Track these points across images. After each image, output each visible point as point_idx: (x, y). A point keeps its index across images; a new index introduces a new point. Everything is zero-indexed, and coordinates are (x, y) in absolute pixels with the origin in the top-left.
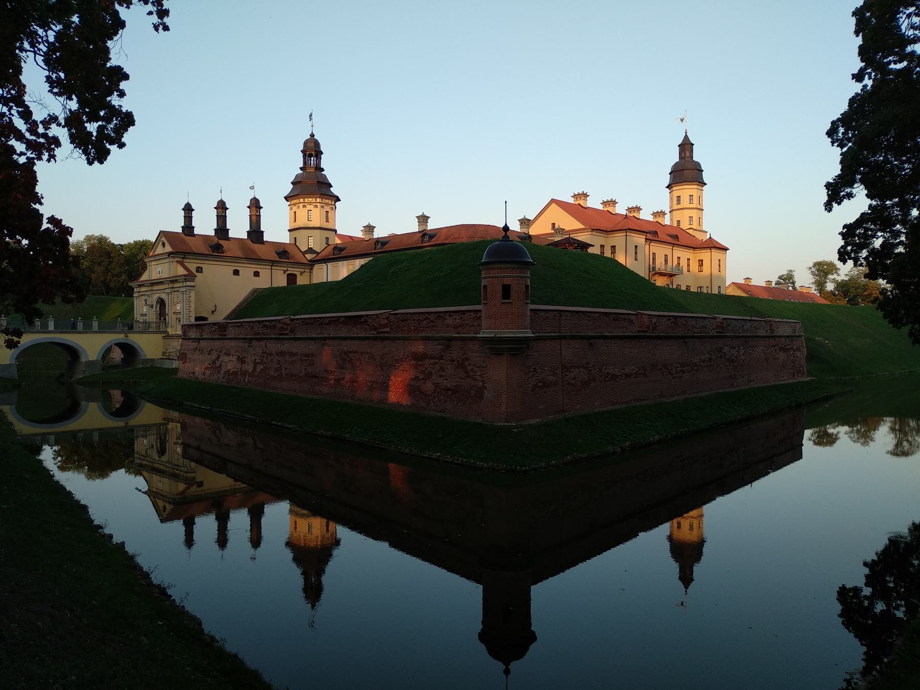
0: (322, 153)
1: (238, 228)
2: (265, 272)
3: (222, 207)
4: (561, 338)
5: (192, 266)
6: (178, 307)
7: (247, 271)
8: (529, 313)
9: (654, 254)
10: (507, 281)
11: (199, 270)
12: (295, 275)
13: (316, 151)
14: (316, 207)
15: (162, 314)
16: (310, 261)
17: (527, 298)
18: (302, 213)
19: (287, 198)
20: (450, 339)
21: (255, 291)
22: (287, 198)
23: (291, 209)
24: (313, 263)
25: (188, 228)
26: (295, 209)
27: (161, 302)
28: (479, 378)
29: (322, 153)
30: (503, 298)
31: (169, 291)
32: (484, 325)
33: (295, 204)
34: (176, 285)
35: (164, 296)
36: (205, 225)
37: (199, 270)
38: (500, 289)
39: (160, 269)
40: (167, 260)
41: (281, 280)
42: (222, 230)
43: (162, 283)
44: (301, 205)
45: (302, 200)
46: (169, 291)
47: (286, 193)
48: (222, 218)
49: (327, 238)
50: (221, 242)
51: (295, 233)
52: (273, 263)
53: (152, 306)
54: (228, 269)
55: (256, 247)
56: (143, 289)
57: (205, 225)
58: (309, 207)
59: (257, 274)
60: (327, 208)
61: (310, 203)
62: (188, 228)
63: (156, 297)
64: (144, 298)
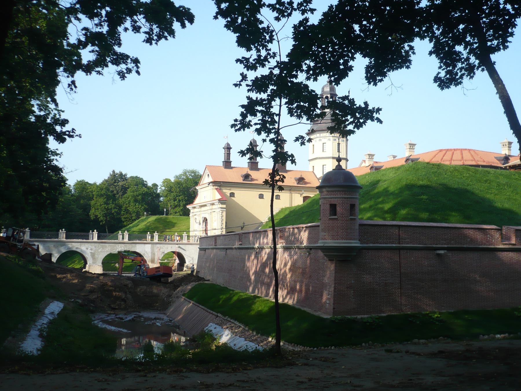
4: (399, 249)
5: (227, 192)
8: (357, 227)
10: (334, 201)
13: (331, 94)
14: (329, 140)
27: (205, 220)
30: (331, 215)
31: (209, 211)
34: (214, 207)
37: (232, 195)
38: (328, 207)
43: (205, 206)
44: (318, 139)
46: (209, 211)
51: (313, 163)
53: (200, 224)
58: (324, 141)
62: (227, 164)
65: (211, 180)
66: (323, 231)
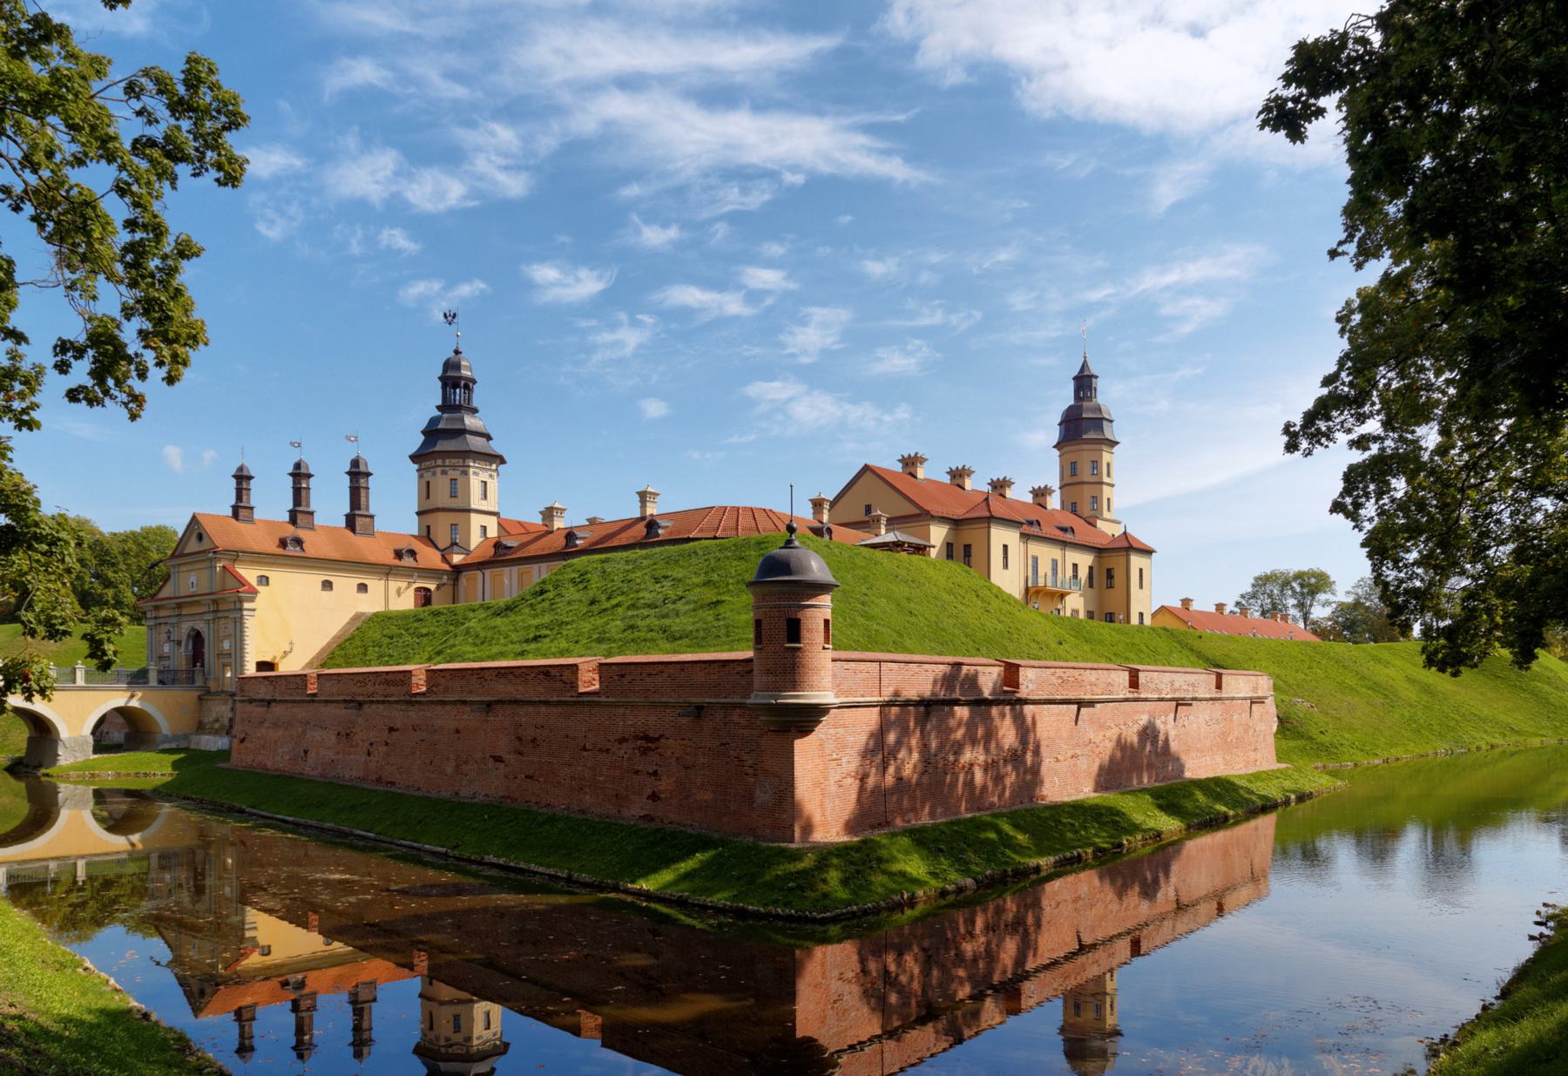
0: (474, 382)
1: (329, 504)
2: (375, 584)
3: (299, 475)
6: (226, 645)
7: (345, 583)
8: (830, 665)
9: (1035, 559)
11: (264, 580)
12: (428, 590)
15: (197, 656)
16: (453, 567)
17: (827, 640)
18: (441, 483)
19: (415, 458)
20: (700, 708)
21: (357, 617)
22: (415, 458)
23: (421, 476)
24: (458, 570)
26: (428, 476)
27: (197, 638)
28: (750, 771)
29: (474, 382)
32: (756, 685)
33: (427, 469)
35: (200, 626)
36: (271, 503)
37: (264, 580)
38: (783, 625)
39: (193, 579)
40: (207, 564)
41: (400, 597)
44: (439, 470)
45: (439, 462)
46: (207, 617)
47: (413, 449)
48: (299, 494)
49: (484, 528)
50: (301, 533)
51: (430, 519)
52: (387, 571)
53: (179, 643)
54: (315, 578)
55: (359, 541)
56: (162, 613)
57: (271, 503)
58: (453, 474)
59: (363, 588)
60: (484, 476)
61: (454, 467)
63: (185, 627)
64: (164, 629)
65: (205, 545)
66: (768, 672)
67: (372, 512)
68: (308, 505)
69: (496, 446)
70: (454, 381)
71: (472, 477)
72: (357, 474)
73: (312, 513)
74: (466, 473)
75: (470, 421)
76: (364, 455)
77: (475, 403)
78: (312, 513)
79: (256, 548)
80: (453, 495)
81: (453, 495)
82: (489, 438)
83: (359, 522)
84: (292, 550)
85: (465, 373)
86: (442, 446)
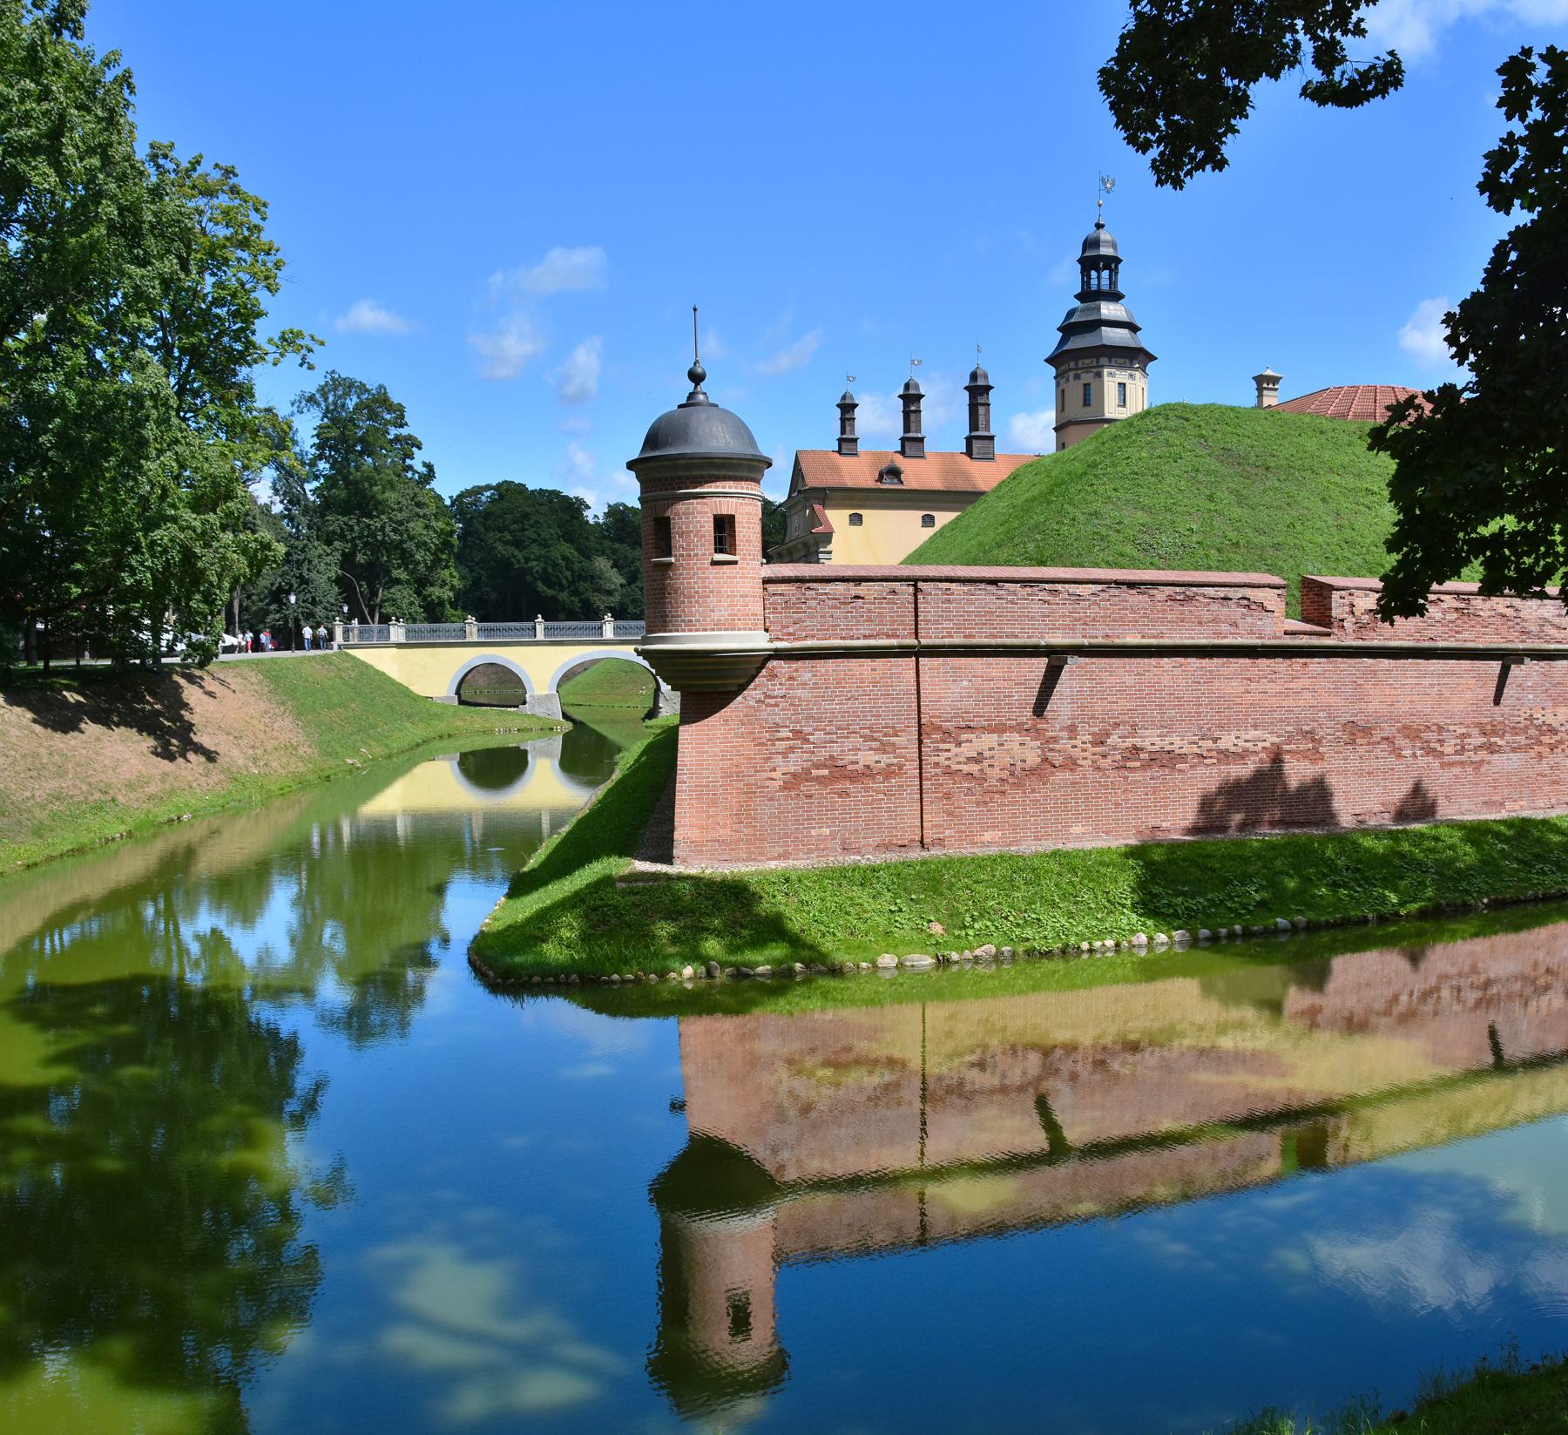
0: (1118, 261)
3: (911, 399)
22: (1049, 361)
25: (847, 444)
29: (1118, 261)
42: (911, 443)
44: (1071, 374)
45: (1072, 365)
47: (1049, 350)
58: (1087, 378)
60: (1122, 376)
61: (1087, 369)
62: (847, 444)
67: (992, 432)
68: (987, 428)
69: (1144, 340)
70: (1095, 261)
71: (1106, 378)
72: (978, 391)
73: (921, 440)
74: (1099, 375)
75: (1108, 310)
76: (985, 367)
77: (1121, 289)
78: (921, 440)
79: (850, 484)
80: (1086, 402)
81: (1086, 402)
82: (1133, 328)
83: (976, 444)
84: (888, 485)
85: (1105, 251)
86: (1076, 343)
